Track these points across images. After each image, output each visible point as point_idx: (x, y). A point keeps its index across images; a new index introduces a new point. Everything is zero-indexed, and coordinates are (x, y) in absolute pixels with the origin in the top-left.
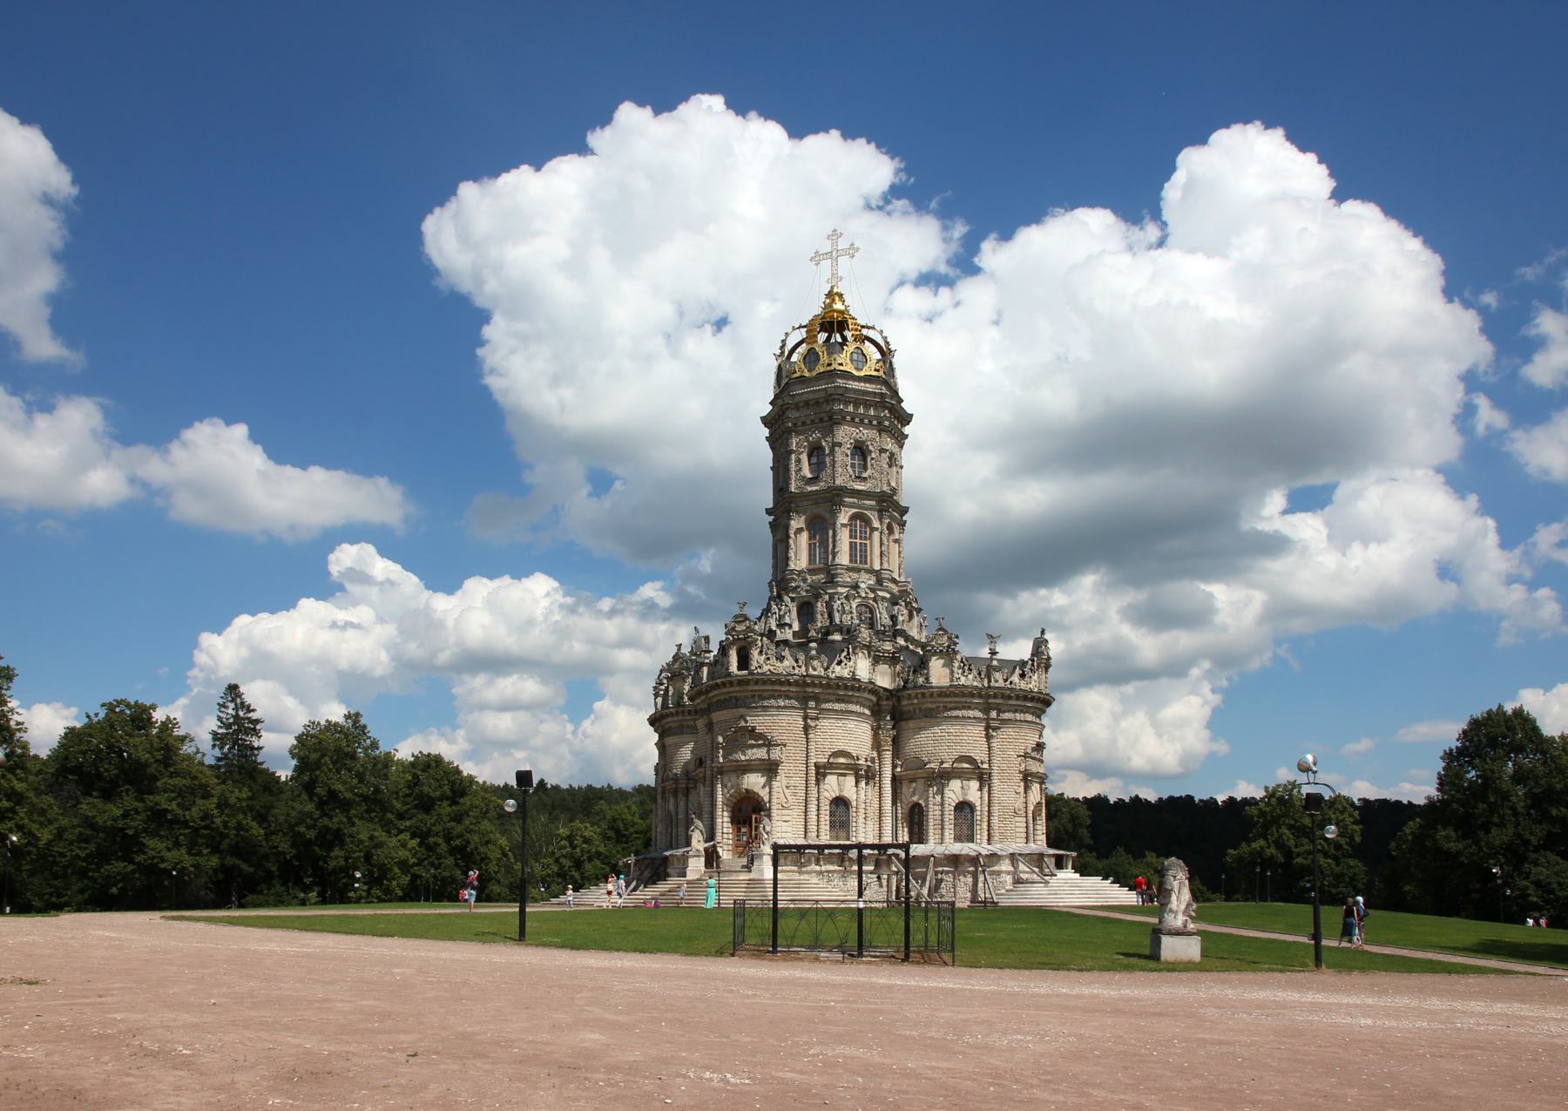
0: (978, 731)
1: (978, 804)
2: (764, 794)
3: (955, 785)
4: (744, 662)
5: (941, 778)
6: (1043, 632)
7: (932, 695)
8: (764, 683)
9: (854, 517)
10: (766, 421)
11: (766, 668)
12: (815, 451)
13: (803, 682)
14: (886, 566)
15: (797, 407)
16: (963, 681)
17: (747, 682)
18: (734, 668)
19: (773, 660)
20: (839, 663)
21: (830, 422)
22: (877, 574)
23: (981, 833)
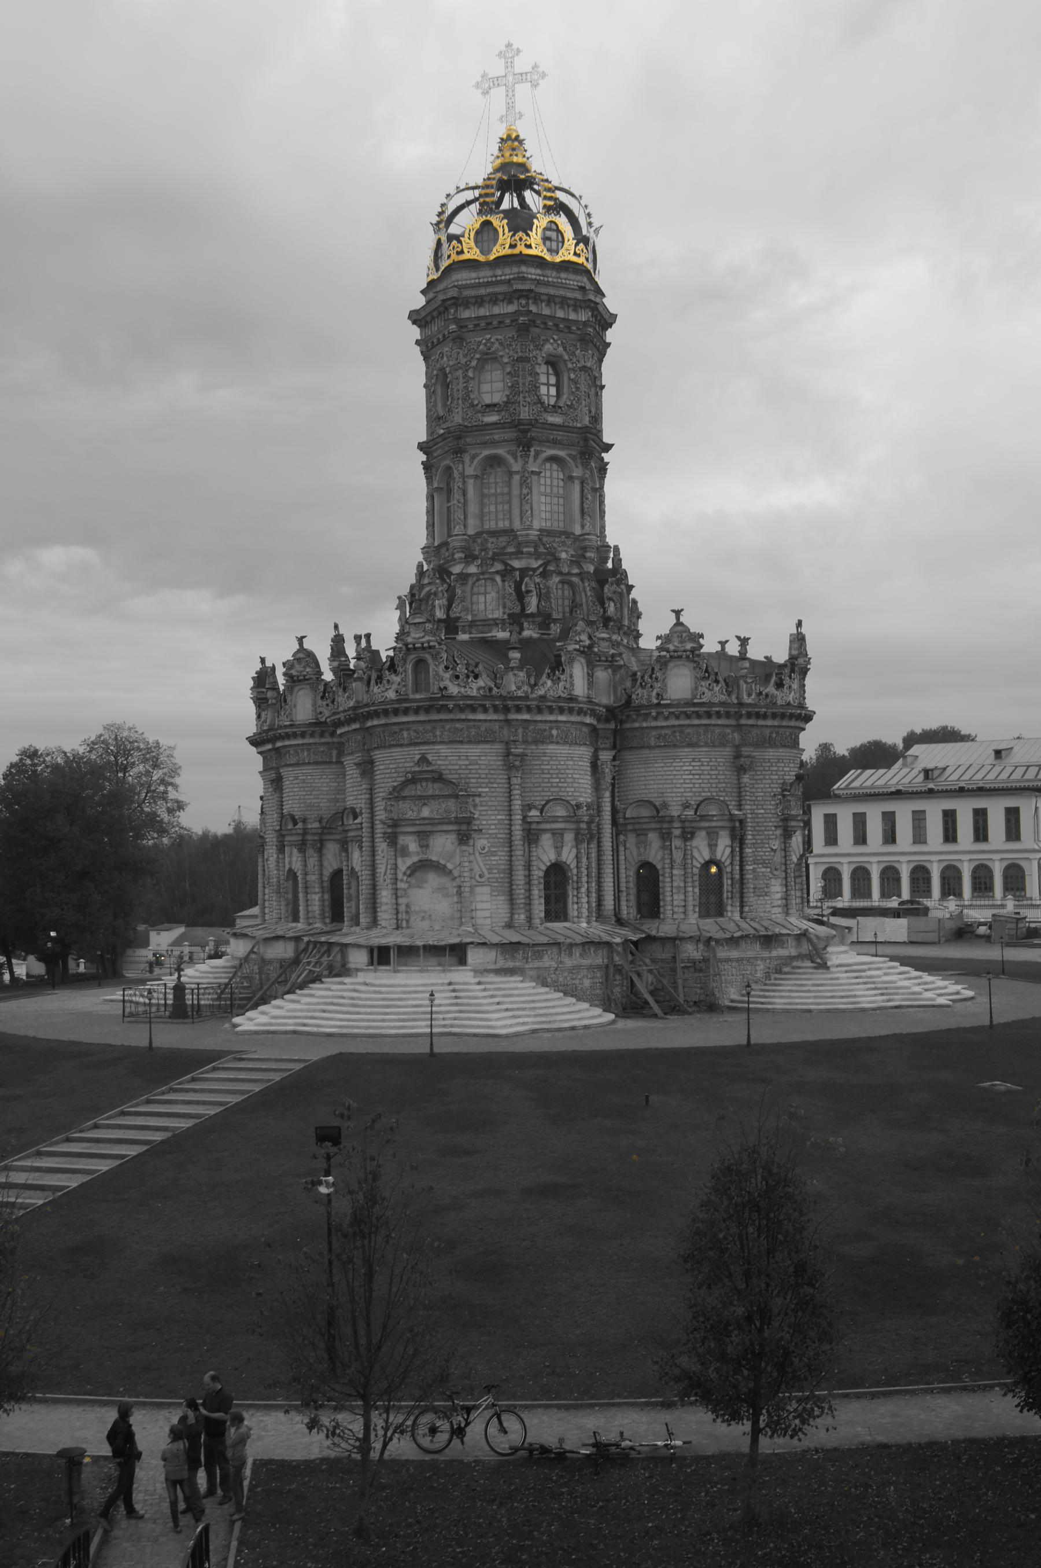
10: (417, 318)
14: (587, 529)
22: (577, 538)
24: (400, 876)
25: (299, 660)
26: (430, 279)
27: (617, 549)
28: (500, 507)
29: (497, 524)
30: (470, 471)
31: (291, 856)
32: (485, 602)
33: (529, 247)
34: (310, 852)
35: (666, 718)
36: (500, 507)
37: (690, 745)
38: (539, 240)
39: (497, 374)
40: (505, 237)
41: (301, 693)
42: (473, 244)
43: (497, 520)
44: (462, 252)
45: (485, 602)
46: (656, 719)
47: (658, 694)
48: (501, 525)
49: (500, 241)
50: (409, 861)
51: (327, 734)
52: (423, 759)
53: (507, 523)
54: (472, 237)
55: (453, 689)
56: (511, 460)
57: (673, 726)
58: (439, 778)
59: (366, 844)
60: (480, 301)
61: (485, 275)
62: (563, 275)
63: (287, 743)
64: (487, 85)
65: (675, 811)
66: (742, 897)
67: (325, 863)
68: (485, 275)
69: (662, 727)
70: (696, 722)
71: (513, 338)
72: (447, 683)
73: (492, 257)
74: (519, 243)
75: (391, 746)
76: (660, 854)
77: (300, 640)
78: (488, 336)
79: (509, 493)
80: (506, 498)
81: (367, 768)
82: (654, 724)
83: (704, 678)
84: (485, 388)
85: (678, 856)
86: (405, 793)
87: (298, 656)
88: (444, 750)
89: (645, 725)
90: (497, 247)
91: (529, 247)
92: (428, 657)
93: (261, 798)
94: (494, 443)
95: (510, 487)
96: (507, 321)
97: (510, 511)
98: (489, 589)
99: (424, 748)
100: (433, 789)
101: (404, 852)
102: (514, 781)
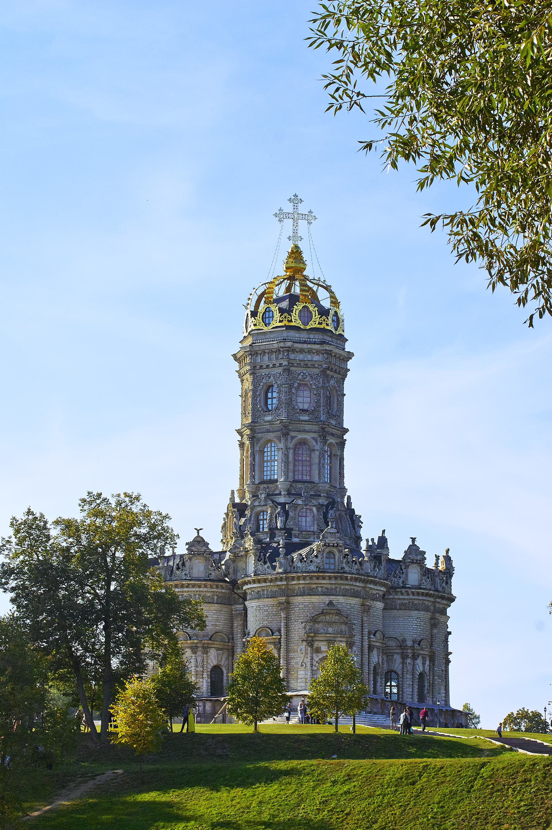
24: (315, 663)
25: (199, 542)
27: (349, 498)
28: (304, 468)
29: (302, 477)
30: (291, 445)
32: (306, 521)
33: (327, 325)
34: (199, 653)
35: (408, 595)
36: (304, 468)
37: (416, 610)
39: (307, 393)
40: (316, 317)
41: (197, 561)
42: (298, 318)
43: (302, 475)
44: (291, 321)
45: (306, 521)
46: (402, 594)
47: (403, 582)
48: (304, 478)
49: (313, 319)
50: (321, 656)
52: (331, 603)
53: (308, 478)
54: (297, 313)
55: (347, 569)
56: (315, 443)
57: (410, 599)
58: (339, 613)
60: (302, 351)
61: (304, 336)
62: (338, 342)
63: (185, 589)
64: (282, 216)
65: (409, 643)
66: (433, 693)
68: (304, 336)
69: (404, 599)
70: (421, 598)
71: (318, 375)
72: (344, 565)
75: (311, 595)
76: (401, 666)
79: (310, 461)
80: (308, 463)
82: (401, 597)
83: (424, 575)
84: (300, 399)
85: (409, 667)
86: (320, 619)
88: (341, 599)
89: (396, 597)
90: (311, 322)
91: (327, 325)
92: (335, 550)
94: (305, 431)
95: (310, 457)
97: (310, 471)
98: (308, 514)
99: (332, 598)
100: (335, 618)
101: (318, 650)
102: (365, 619)
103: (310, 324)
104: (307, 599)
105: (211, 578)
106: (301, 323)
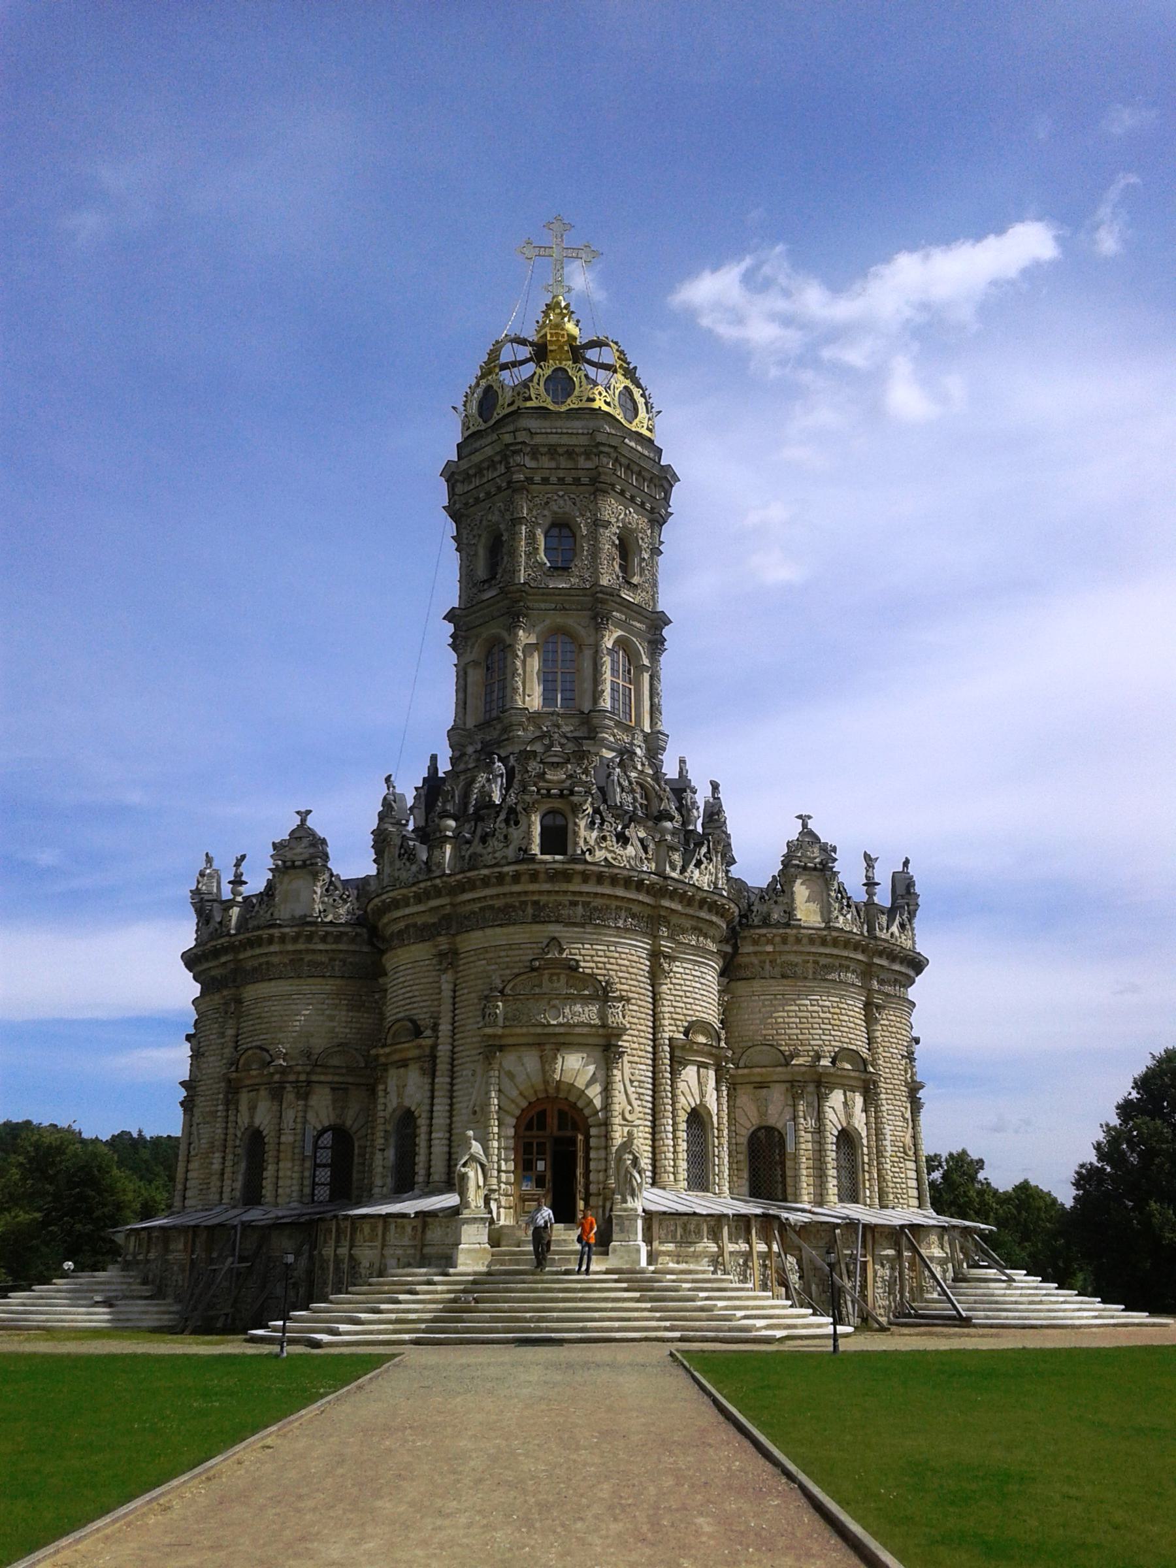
0: (854, 1008)
1: (864, 1134)
2: (594, 1093)
3: (836, 1098)
4: (556, 838)
5: (815, 1085)
6: (906, 863)
7: (798, 941)
8: (600, 878)
9: (619, 642)
11: (600, 855)
12: (561, 529)
13: (661, 889)
15: (535, 454)
16: (840, 923)
17: (566, 876)
18: (536, 849)
19: (612, 842)
20: (698, 864)
21: (597, 486)
23: (869, 1191)
26: (470, 432)
31: (253, 1108)
38: (617, 403)
44: (530, 399)
49: (576, 393)
51: (330, 939)
59: (442, 1066)
67: (311, 1116)
73: (563, 409)
74: (597, 397)
77: (304, 815)
78: (561, 493)
81: (449, 959)
87: (296, 835)
90: (573, 398)
93: (189, 1038)
96: (585, 480)
103: (569, 401)
104: (497, 936)
105: (328, 920)
106: (549, 399)
